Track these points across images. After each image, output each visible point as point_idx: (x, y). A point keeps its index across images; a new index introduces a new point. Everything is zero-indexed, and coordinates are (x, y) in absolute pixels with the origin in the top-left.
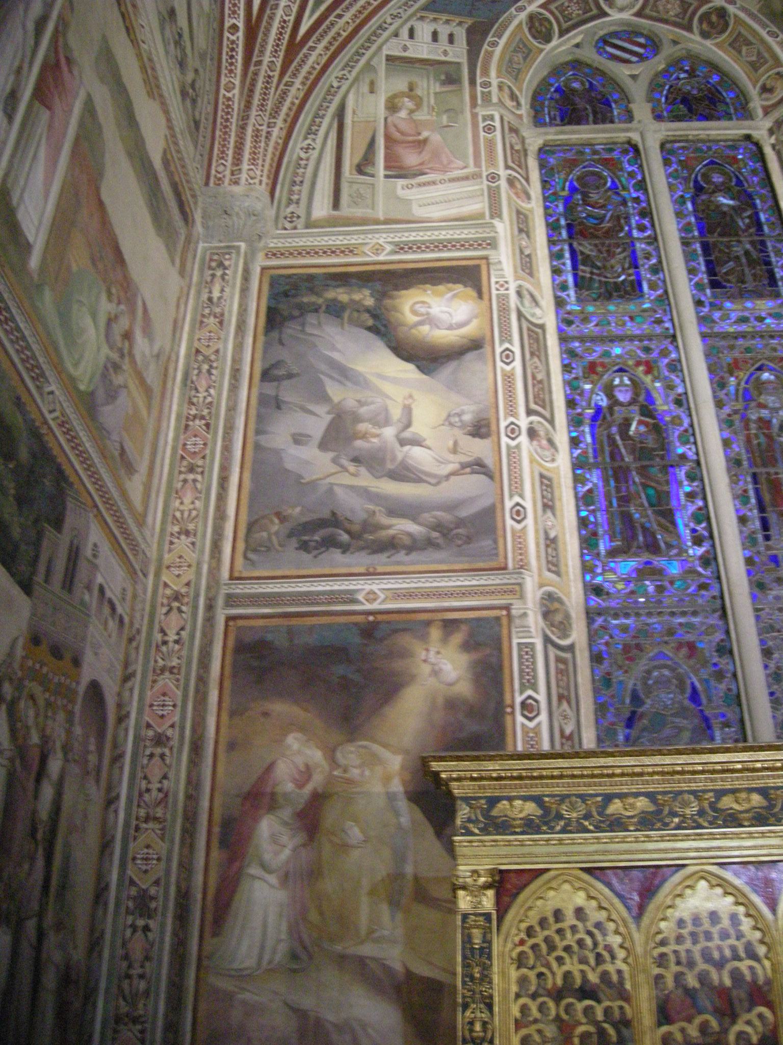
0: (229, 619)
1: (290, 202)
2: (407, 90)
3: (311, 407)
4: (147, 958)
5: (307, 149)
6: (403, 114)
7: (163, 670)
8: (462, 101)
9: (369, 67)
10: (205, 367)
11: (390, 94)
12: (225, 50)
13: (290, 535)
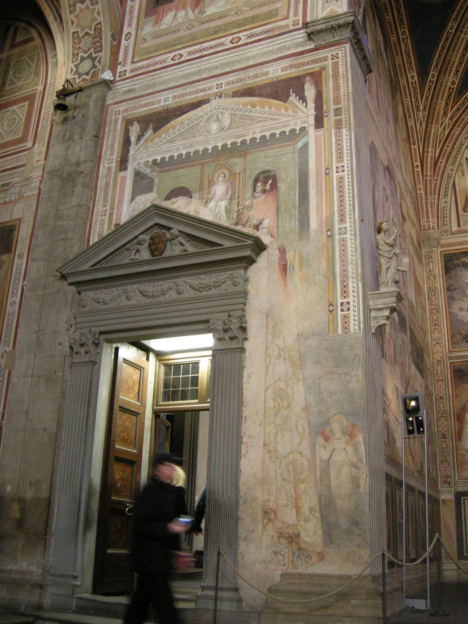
0: (450, 363)
1: (444, 225)
3: (463, 299)
4: (447, 448)
5: (446, 202)
7: (439, 380)
9: (460, 164)
10: (433, 293)
12: (416, 175)
13: (463, 338)
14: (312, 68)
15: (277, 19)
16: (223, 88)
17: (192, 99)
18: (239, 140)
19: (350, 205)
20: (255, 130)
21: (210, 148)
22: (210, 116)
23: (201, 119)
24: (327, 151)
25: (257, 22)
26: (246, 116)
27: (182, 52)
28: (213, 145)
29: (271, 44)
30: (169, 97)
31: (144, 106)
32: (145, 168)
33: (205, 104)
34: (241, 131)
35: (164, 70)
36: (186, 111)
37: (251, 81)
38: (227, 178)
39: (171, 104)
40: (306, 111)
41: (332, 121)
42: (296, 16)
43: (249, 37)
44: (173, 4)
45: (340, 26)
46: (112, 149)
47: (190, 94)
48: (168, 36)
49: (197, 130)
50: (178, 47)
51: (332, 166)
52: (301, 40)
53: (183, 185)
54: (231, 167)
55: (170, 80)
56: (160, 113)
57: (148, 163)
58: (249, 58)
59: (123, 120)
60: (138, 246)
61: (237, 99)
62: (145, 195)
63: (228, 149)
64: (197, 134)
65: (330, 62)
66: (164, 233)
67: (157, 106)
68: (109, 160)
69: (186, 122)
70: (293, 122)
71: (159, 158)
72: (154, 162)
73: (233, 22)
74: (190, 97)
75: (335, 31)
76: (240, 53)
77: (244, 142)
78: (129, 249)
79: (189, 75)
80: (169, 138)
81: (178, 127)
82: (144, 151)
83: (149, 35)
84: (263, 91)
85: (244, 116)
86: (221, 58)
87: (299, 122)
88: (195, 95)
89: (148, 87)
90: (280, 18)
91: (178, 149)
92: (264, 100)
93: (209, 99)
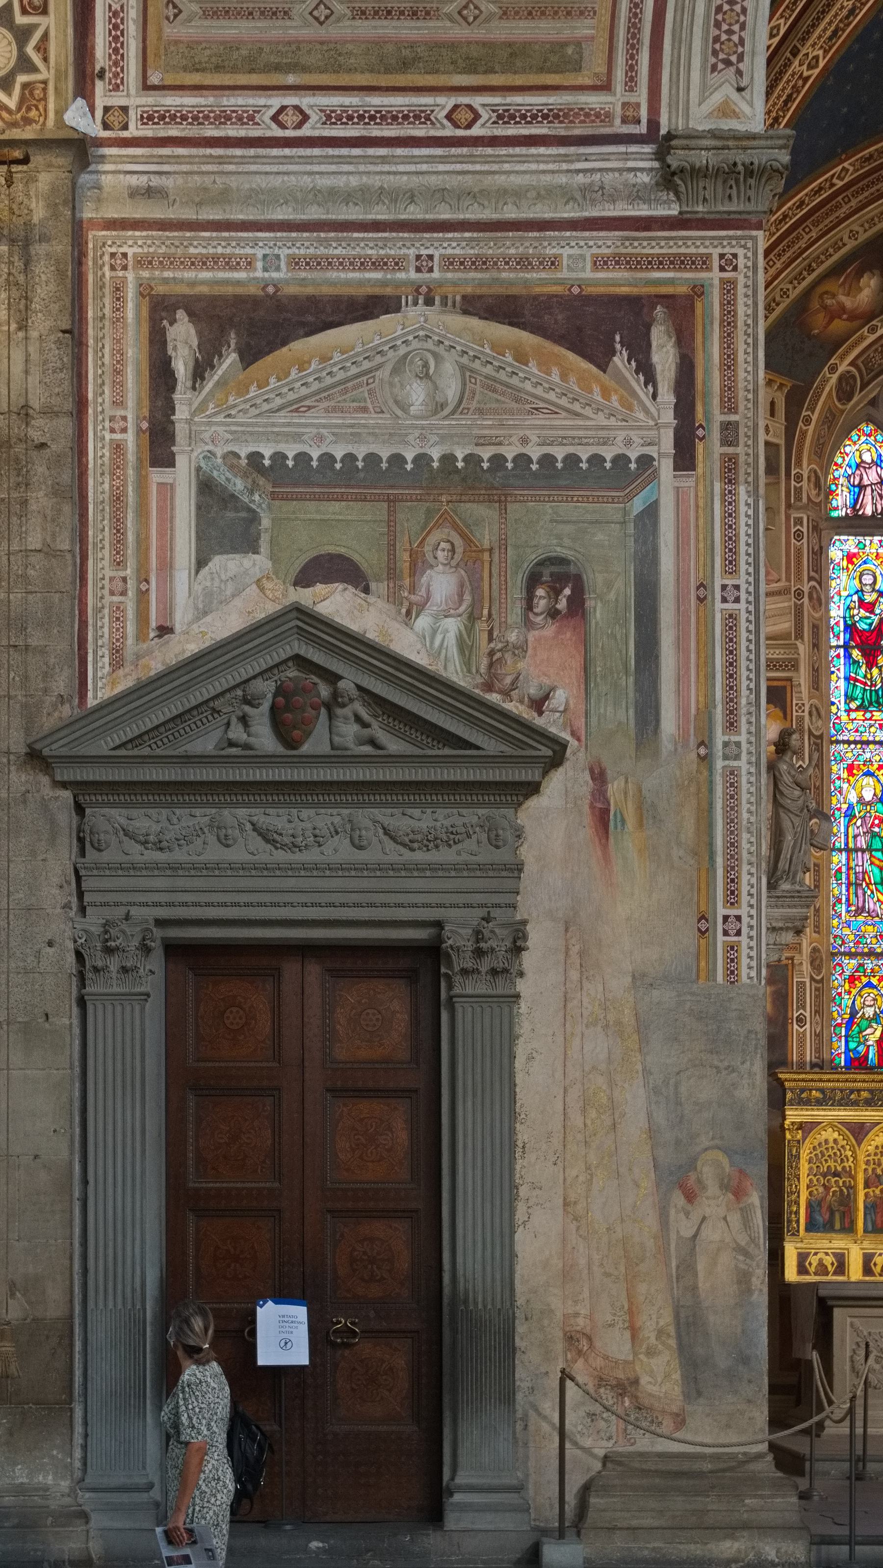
16: (436, 275)
17: (348, 283)
18: (486, 453)
19: (751, 690)
21: (409, 456)
22: (406, 356)
23: (379, 359)
24: (701, 537)
26: (502, 383)
31: (203, 262)
32: (230, 476)
33: (387, 312)
34: (490, 427)
37: (512, 275)
38: (458, 556)
39: (287, 282)
40: (653, 410)
41: (716, 456)
46: (119, 385)
47: (342, 263)
49: (370, 392)
51: (713, 583)
53: (342, 551)
54: (468, 526)
55: (273, 197)
56: (255, 302)
57: (235, 461)
58: (503, 194)
60: (247, 708)
61: (475, 322)
62: (237, 556)
63: (457, 471)
64: (370, 407)
66: (315, 684)
67: (241, 275)
68: (112, 419)
69: (337, 357)
70: (621, 435)
71: (267, 451)
74: (343, 275)
76: (478, 167)
77: (498, 460)
78: (218, 712)
79: (333, 195)
80: (291, 396)
81: (313, 366)
82: (220, 418)
84: (546, 317)
85: (495, 380)
86: (424, 167)
89: (204, 197)
91: (321, 438)
92: (549, 346)
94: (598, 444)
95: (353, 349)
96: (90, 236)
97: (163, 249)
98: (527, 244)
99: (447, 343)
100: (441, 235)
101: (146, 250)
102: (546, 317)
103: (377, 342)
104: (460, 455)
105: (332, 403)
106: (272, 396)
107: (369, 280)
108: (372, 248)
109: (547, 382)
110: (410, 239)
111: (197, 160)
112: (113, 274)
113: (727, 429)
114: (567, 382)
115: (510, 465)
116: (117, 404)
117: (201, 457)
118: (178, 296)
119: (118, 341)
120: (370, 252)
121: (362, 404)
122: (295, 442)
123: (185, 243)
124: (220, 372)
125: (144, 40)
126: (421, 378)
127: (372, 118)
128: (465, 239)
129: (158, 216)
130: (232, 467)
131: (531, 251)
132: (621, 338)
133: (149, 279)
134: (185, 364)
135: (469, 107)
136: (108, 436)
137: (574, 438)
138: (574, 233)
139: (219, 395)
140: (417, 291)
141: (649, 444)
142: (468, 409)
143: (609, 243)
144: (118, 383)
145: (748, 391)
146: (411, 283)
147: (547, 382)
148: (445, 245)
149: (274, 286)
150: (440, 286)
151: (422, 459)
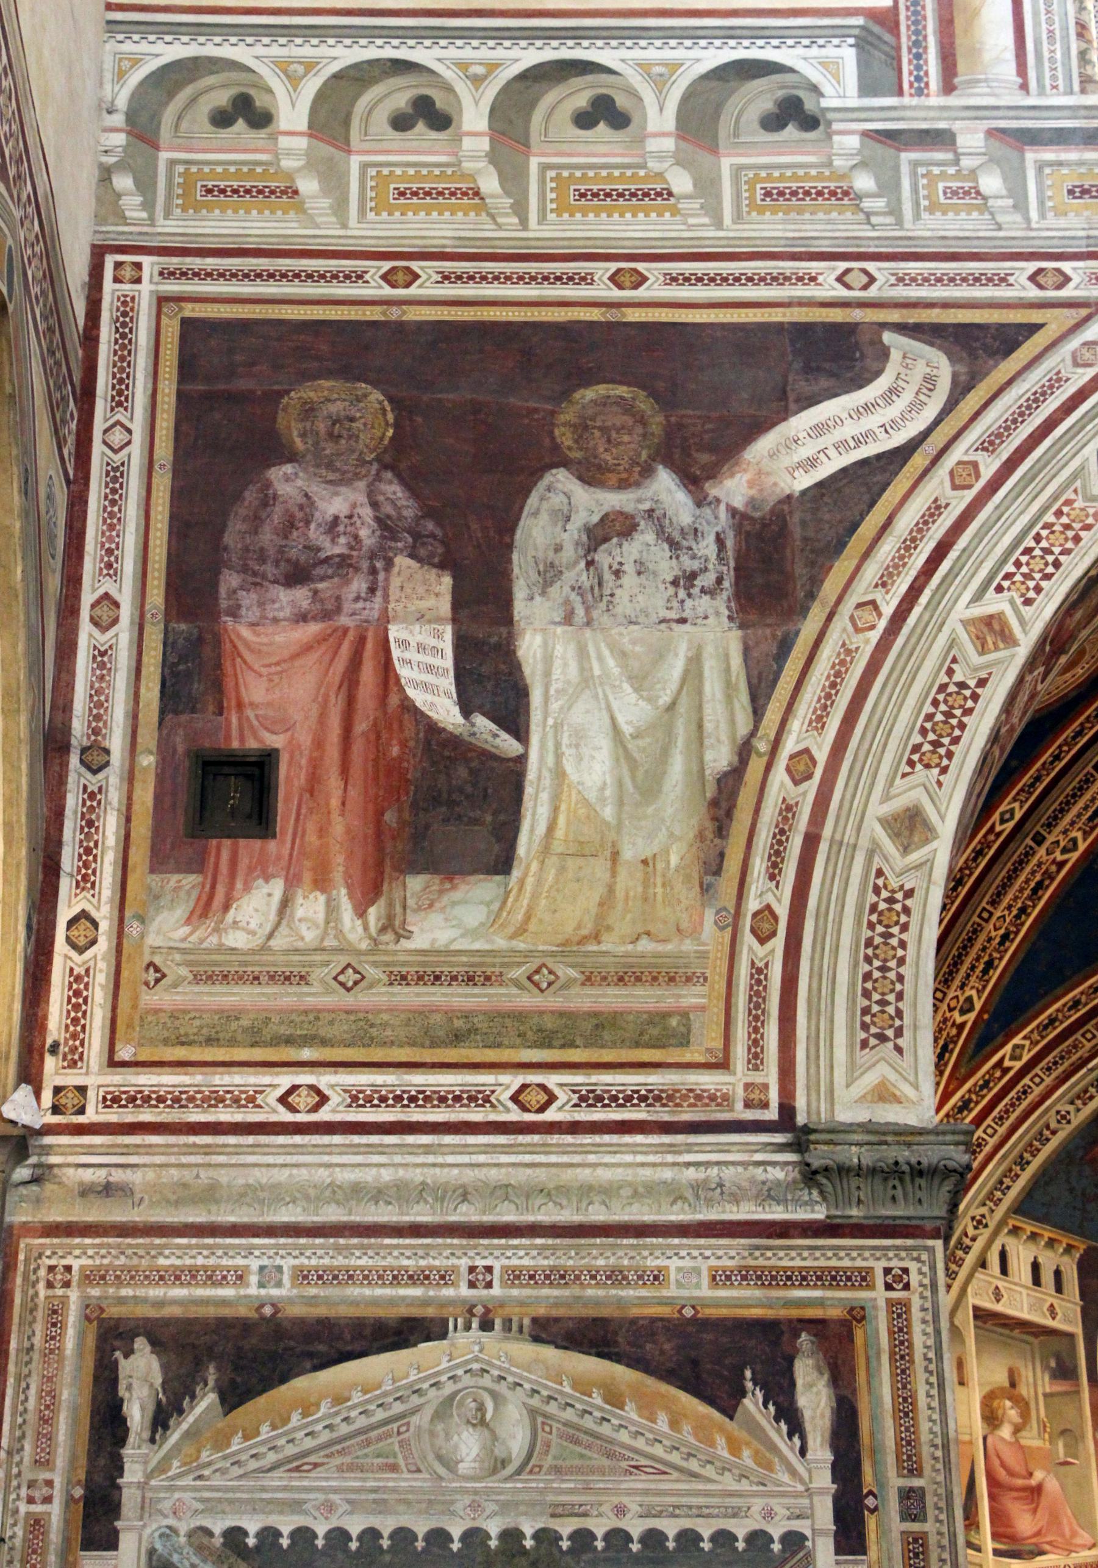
2: (1007, 1384)
6: (1006, 1432)
8: (1080, 1409)
11: (987, 1389)
14: (820, 1303)
15: (688, 1057)
16: (496, 1291)
17: (375, 1302)
18: (566, 1528)
20: (625, 1500)
21: (456, 1532)
22: (452, 1397)
23: (415, 1400)
25: (614, 1045)
27: (325, 1080)
28: (469, 1524)
29: (670, 1158)
30: (279, 1269)
31: (177, 1276)
33: (428, 1339)
34: (571, 1492)
35: (250, 1139)
36: (357, 1347)
37: (601, 1292)
39: (290, 1301)
40: (801, 1469)
41: (896, 1536)
42: (756, 1068)
43: (583, 1099)
44: (272, 845)
45: (918, 1172)
47: (367, 1277)
48: (257, 990)
50: (306, 1054)
52: (778, 1174)
55: (277, 1194)
56: (245, 1326)
57: (205, 1540)
58: (587, 1191)
59: (88, 1319)
61: (549, 1353)
63: (524, 1552)
65: (879, 1296)
68: (31, 1485)
69: (357, 1397)
70: (758, 1504)
71: (252, 1526)
72: (235, 1535)
73: (520, 1016)
74: (367, 1292)
75: (901, 1180)
76: (553, 1159)
77: (582, 1538)
79: (357, 1191)
80: (291, 1450)
81: (323, 1410)
82: (188, 1481)
83: (178, 957)
84: (648, 1346)
85: (578, 1428)
86: (482, 1158)
87: (778, 1506)
88: (388, 1292)
89: (184, 1194)
90: (701, 1059)
92: (652, 1384)
93: (445, 1322)
94: (725, 1516)
95: (379, 1387)
96: (22, 1246)
97: (122, 1260)
98: (621, 1253)
99: (510, 1379)
100: (503, 1241)
101: (98, 1262)
102: (648, 1346)
103: (412, 1378)
104: (528, 1530)
105: (347, 1460)
106: (263, 1449)
107: (404, 1298)
108: (409, 1258)
109: (651, 1431)
110: (462, 1247)
111: (176, 1150)
112: (50, 1292)
113: (909, 1498)
114: (679, 1431)
115: (600, 1545)
116: (41, 1464)
117: (156, 1534)
118: (138, 1319)
119: (50, 1379)
120: (405, 1262)
121: (391, 1461)
122: (293, 1512)
123: (153, 1253)
124: (191, 1419)
125: (114, 1009)
126: (474, 1425)
127: (413, 1099)
128: (536, 1247)
129: (118, 1219)
130: (200, 1549)
131: (626, 1262)
132: (753, 1373)
133: (99, 1298)
134: (143, 1409)
135: (543, 1087)
136: (23, 1508)
137: (690, 1507)
138: (685, 1241)
139: (188, 1449)
140: (470, 1312)
141: (798, 1517)
142: (540, 1467)
143: (733, 1253)
144: (45, 1435)
145: (936, 1446)
146: (464, 1301)
147: (651, 1431)
148: (509, 1253)
149: (273, 1305)
150: (501, 1306)
151: (473, 1536)
